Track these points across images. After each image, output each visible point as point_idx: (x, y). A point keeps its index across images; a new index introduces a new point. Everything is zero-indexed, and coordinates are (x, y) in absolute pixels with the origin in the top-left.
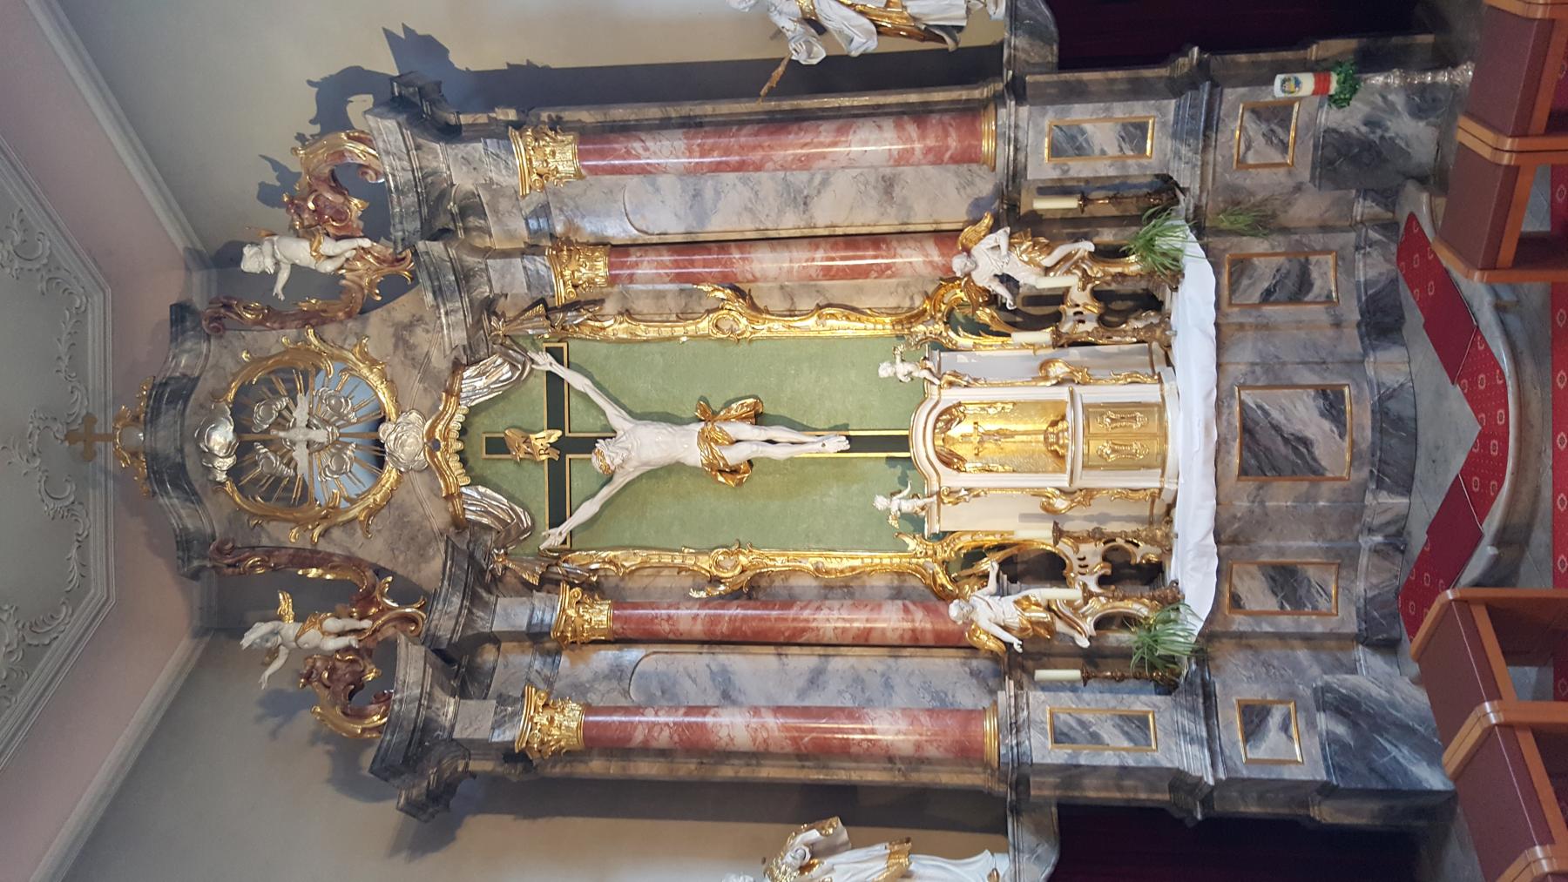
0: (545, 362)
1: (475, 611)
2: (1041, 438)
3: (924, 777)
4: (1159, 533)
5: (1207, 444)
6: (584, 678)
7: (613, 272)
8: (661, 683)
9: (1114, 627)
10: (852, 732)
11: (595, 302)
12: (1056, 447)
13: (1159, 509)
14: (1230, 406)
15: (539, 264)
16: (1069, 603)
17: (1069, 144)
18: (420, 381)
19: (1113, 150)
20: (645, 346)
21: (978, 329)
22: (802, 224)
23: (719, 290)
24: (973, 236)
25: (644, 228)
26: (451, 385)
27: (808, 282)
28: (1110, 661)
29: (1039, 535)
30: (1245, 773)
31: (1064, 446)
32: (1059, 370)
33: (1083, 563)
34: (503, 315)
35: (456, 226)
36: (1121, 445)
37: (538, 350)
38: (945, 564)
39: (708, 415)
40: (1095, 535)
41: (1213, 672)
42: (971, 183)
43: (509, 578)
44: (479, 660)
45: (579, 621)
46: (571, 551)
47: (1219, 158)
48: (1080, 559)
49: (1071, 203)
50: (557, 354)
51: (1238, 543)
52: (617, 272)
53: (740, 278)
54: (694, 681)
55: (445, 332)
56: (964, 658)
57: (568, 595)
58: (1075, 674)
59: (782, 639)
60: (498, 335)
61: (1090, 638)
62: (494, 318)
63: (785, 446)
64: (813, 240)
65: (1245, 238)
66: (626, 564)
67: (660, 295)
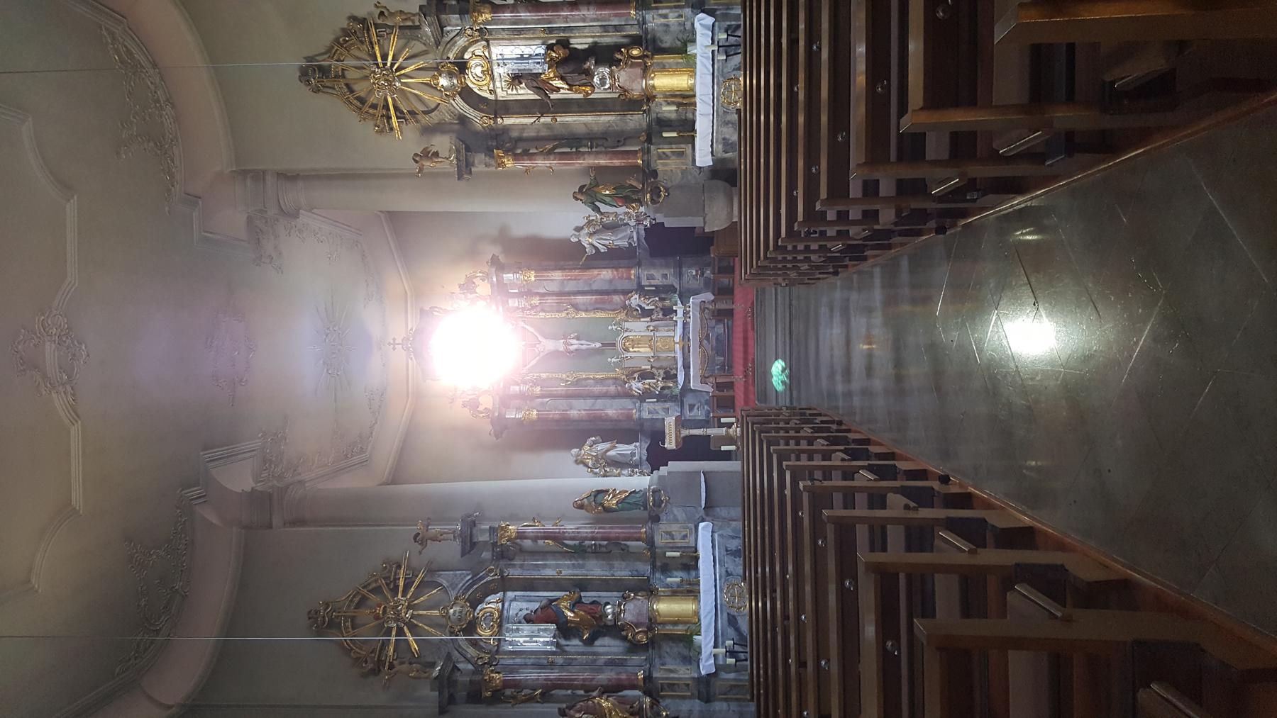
30: (688, 418)
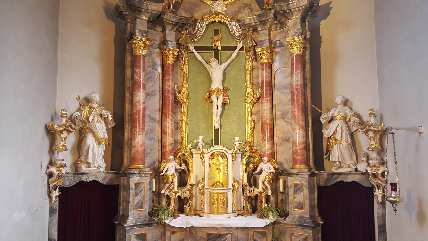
0: (240, 45)
1: (172, 25)
2: (218, 181)
3: (126, 148)
4: (192, 212)
5: (216, 225)
6: (153, 55)
7: (264, 65)
8: (151, 77)
9: (167, 200)
10: (139, 129)
11: (256, 59)
12: (216, 185)
13: (199, 212)
14: (226, 231)
15: (267, 44)
16: (173, 188)
17: (298, 188)
18: (235, 11)
19: (296, 200)
20: (244, 73)
21: (248, 164)
22: (277, 117)
23: (259, 94)
24: (273, 163)
25: (276, 73)
26: (234, 19)
27: (261, 118)
28: (158, 199)
29: (192, 180)
30: (127, 235)
31: (216, 187)
32: (236, 185)
33: (184, 192)
34: (253, 34)
35: (277, 21)
36: (216, 202)
37: (243, 44)
38: (184, 155)
39: (225, 90)
40: (192, 195)
41: (155, 226)
42: (287, 162)
43: (180, 35)
44: (158, 26)
45: (168, 54)
46: (188, 52)
47: (293, 229)
48: (185, 191)
49: (281, 189)
50: (242, 49)
51: (189, 233)
52: (264, 66)
53: (262, 100)
54: (152, 86)
55: (249, 18)
56: (158, 160)
57: (176, 51)
58: (154, 189)
59: (163, 110)
60: (247, 33)
61: (164, 194)
62: (252, 31)
63: (216, 111)
64: (272, 119)
65: (272, 235)
66: (184, 68)
67: (258, 78)
